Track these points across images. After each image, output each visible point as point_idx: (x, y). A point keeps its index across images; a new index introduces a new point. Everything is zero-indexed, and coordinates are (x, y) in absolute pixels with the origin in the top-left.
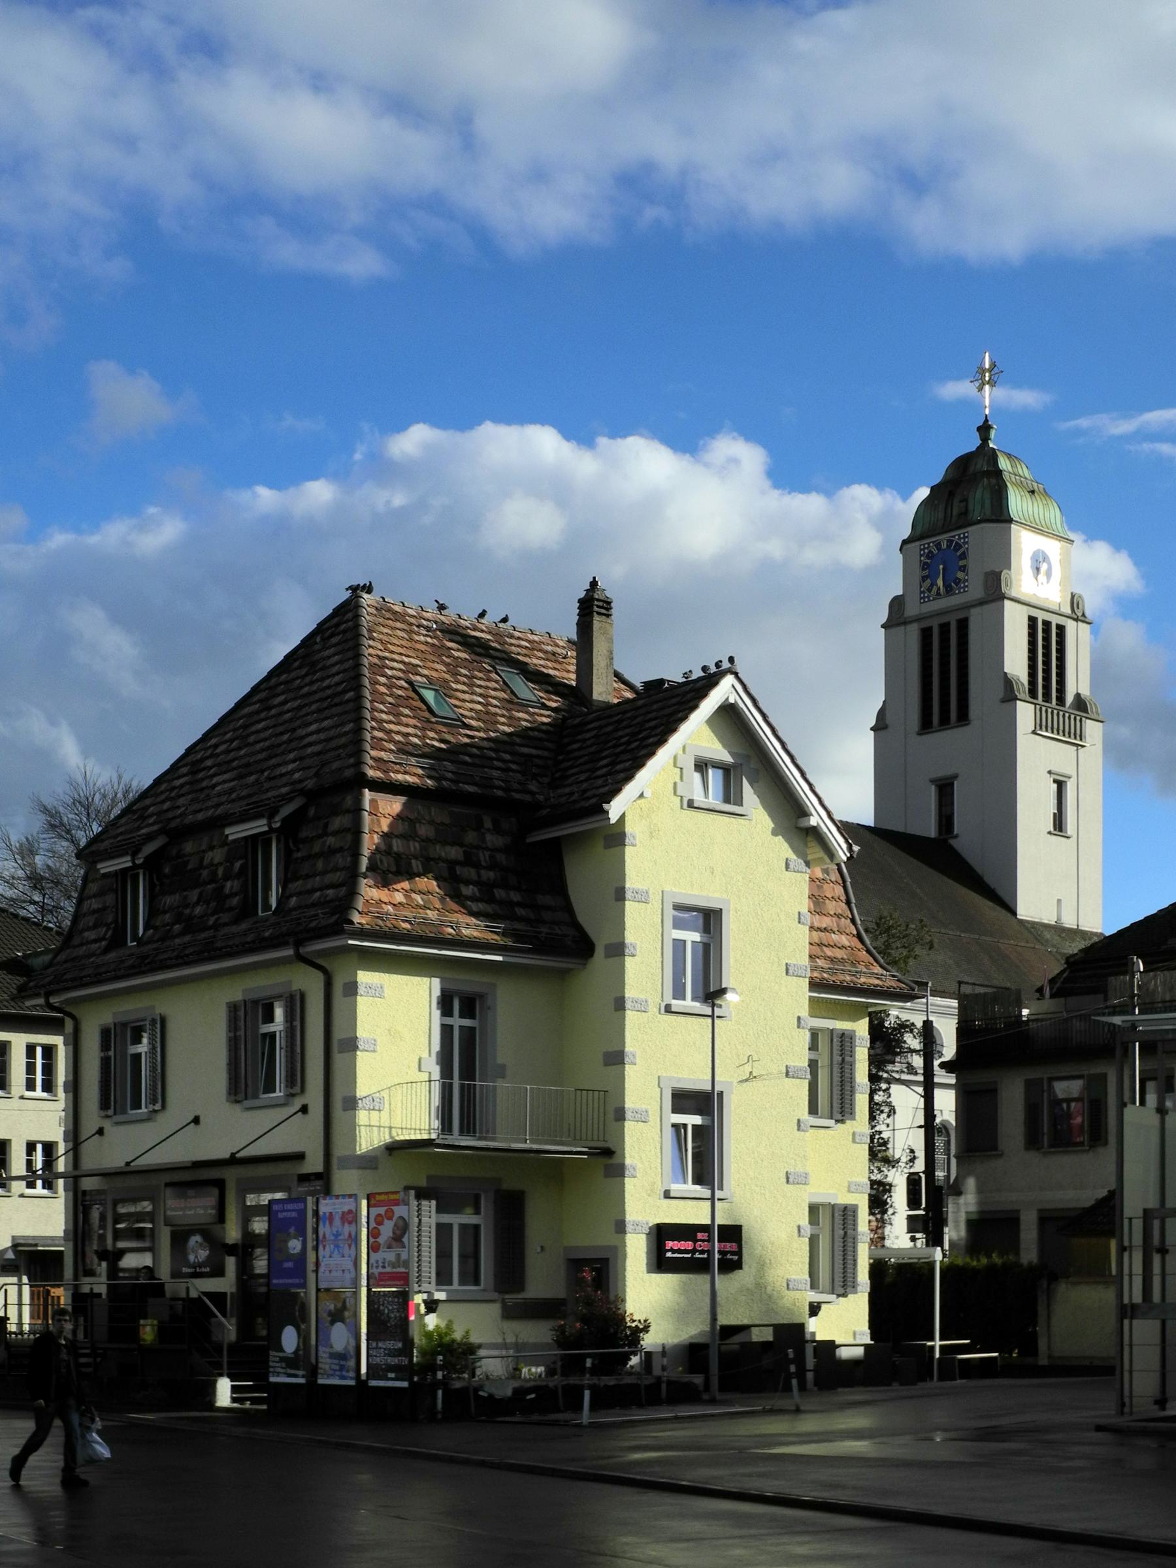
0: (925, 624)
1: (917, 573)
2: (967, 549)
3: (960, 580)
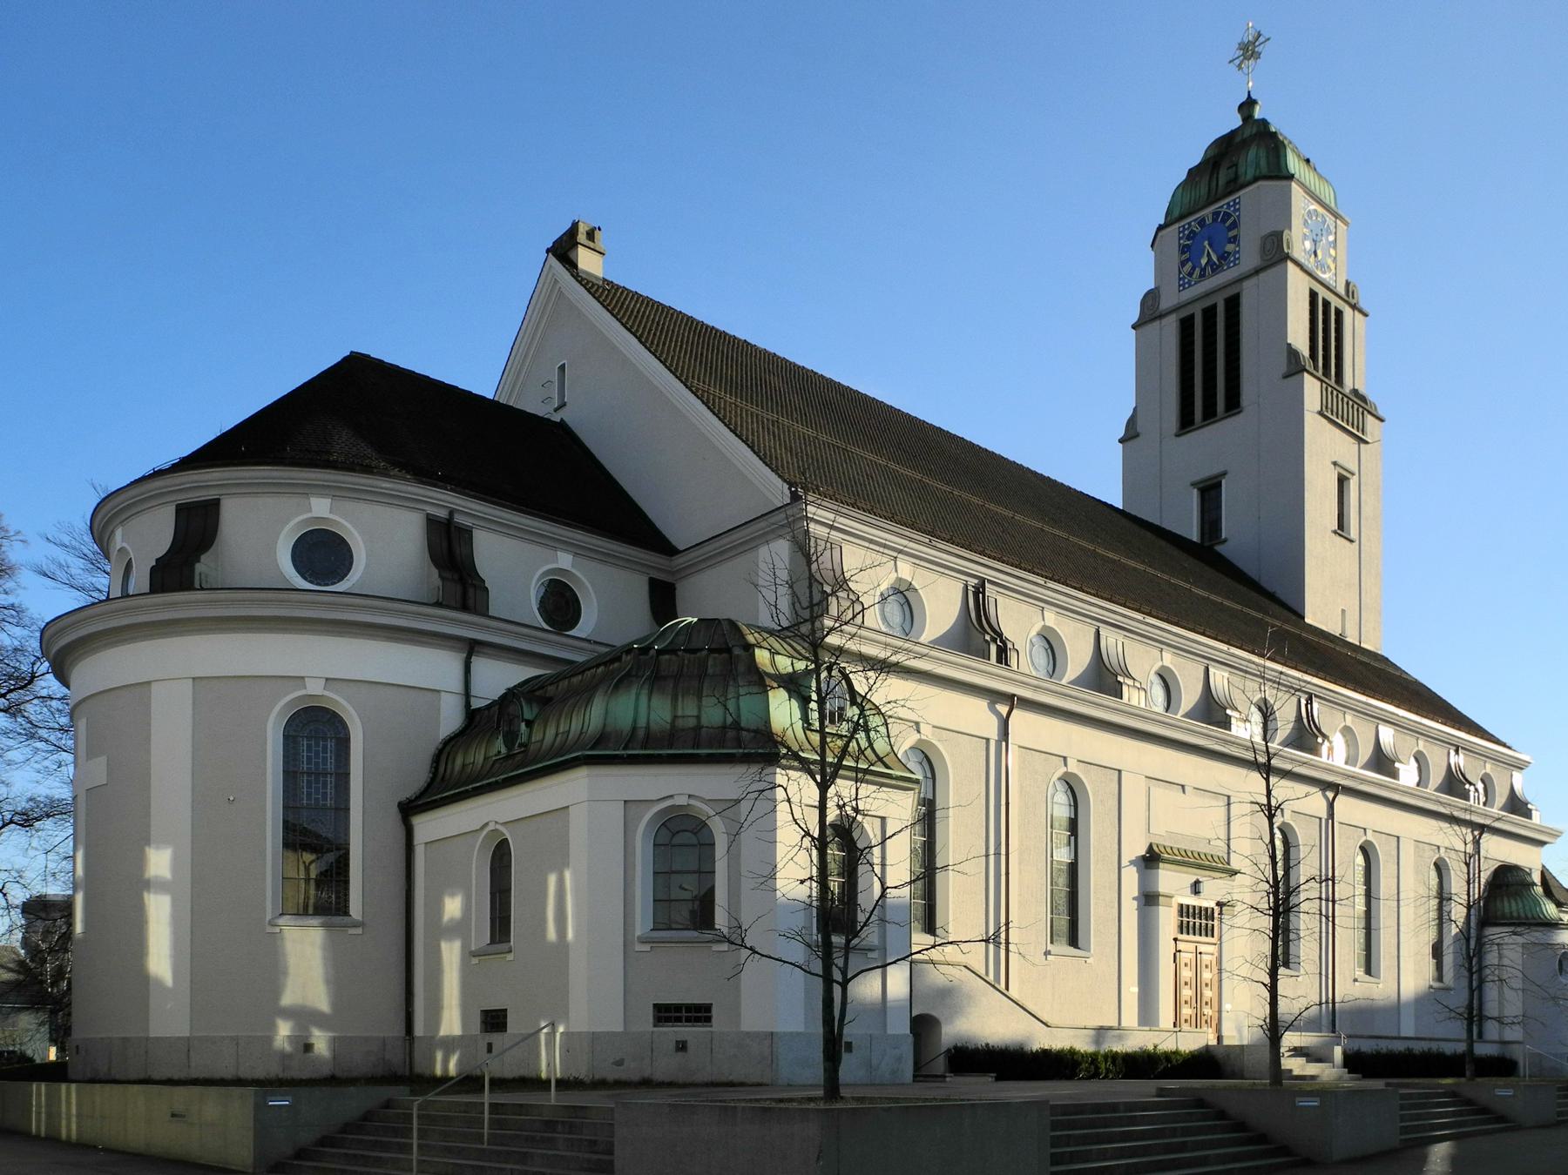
0: (1184, 313)
1: (1174, 256)
2: (1239, 216)
3: (1229, 253)
